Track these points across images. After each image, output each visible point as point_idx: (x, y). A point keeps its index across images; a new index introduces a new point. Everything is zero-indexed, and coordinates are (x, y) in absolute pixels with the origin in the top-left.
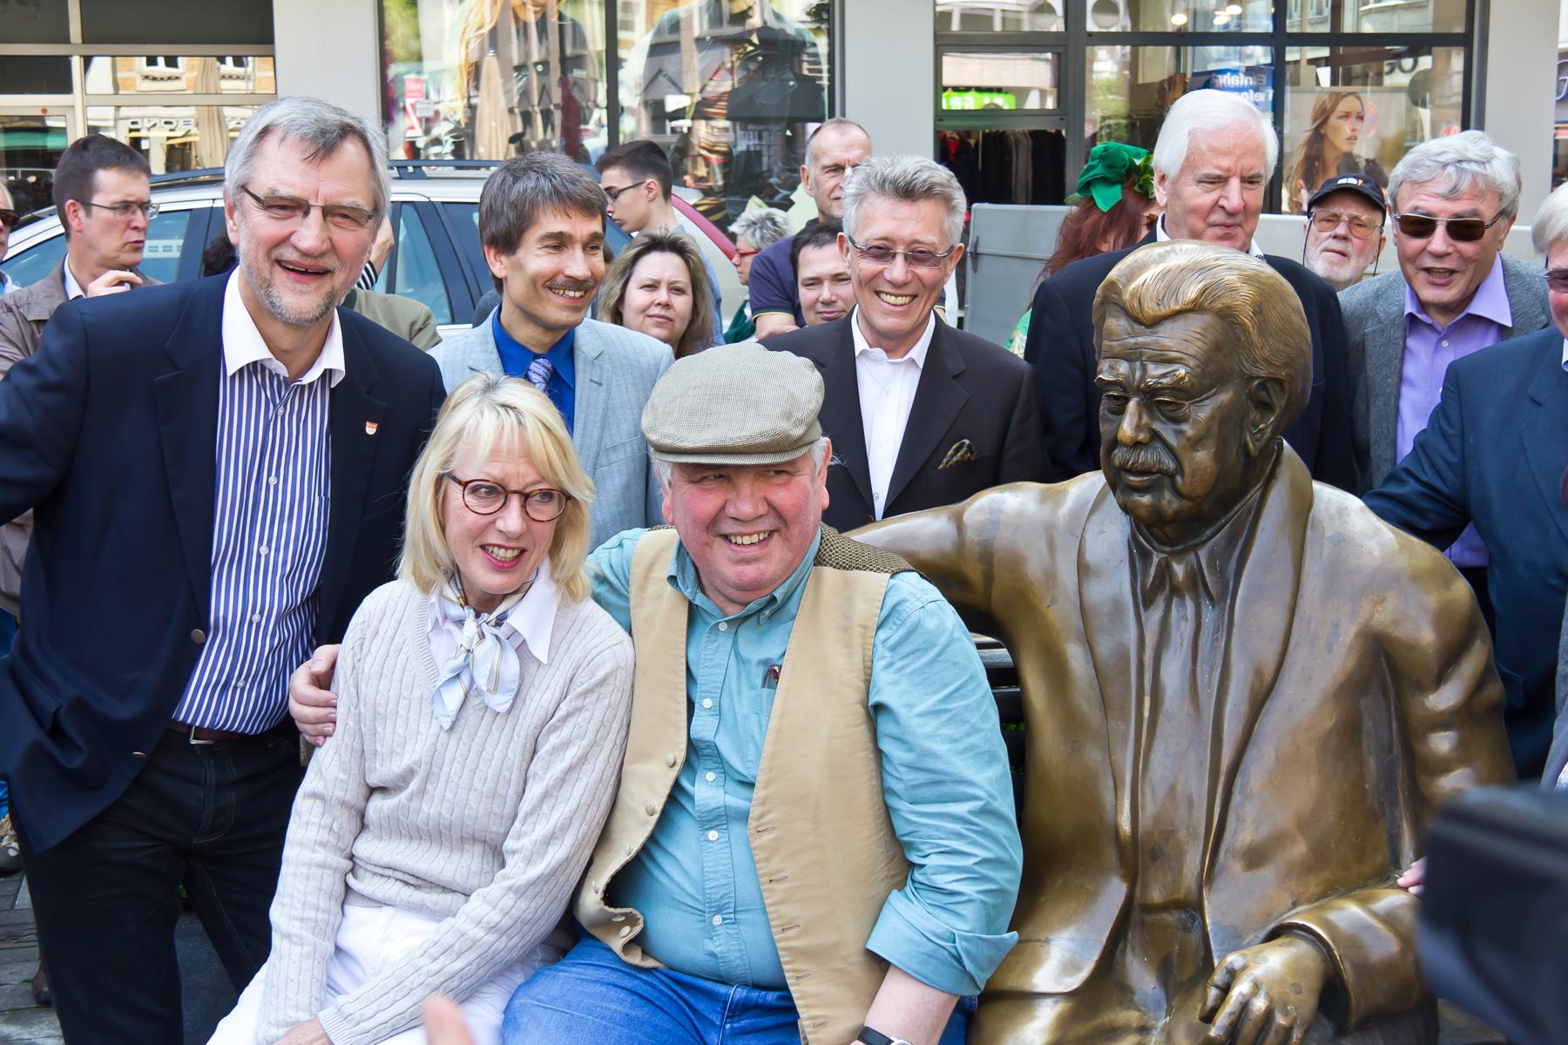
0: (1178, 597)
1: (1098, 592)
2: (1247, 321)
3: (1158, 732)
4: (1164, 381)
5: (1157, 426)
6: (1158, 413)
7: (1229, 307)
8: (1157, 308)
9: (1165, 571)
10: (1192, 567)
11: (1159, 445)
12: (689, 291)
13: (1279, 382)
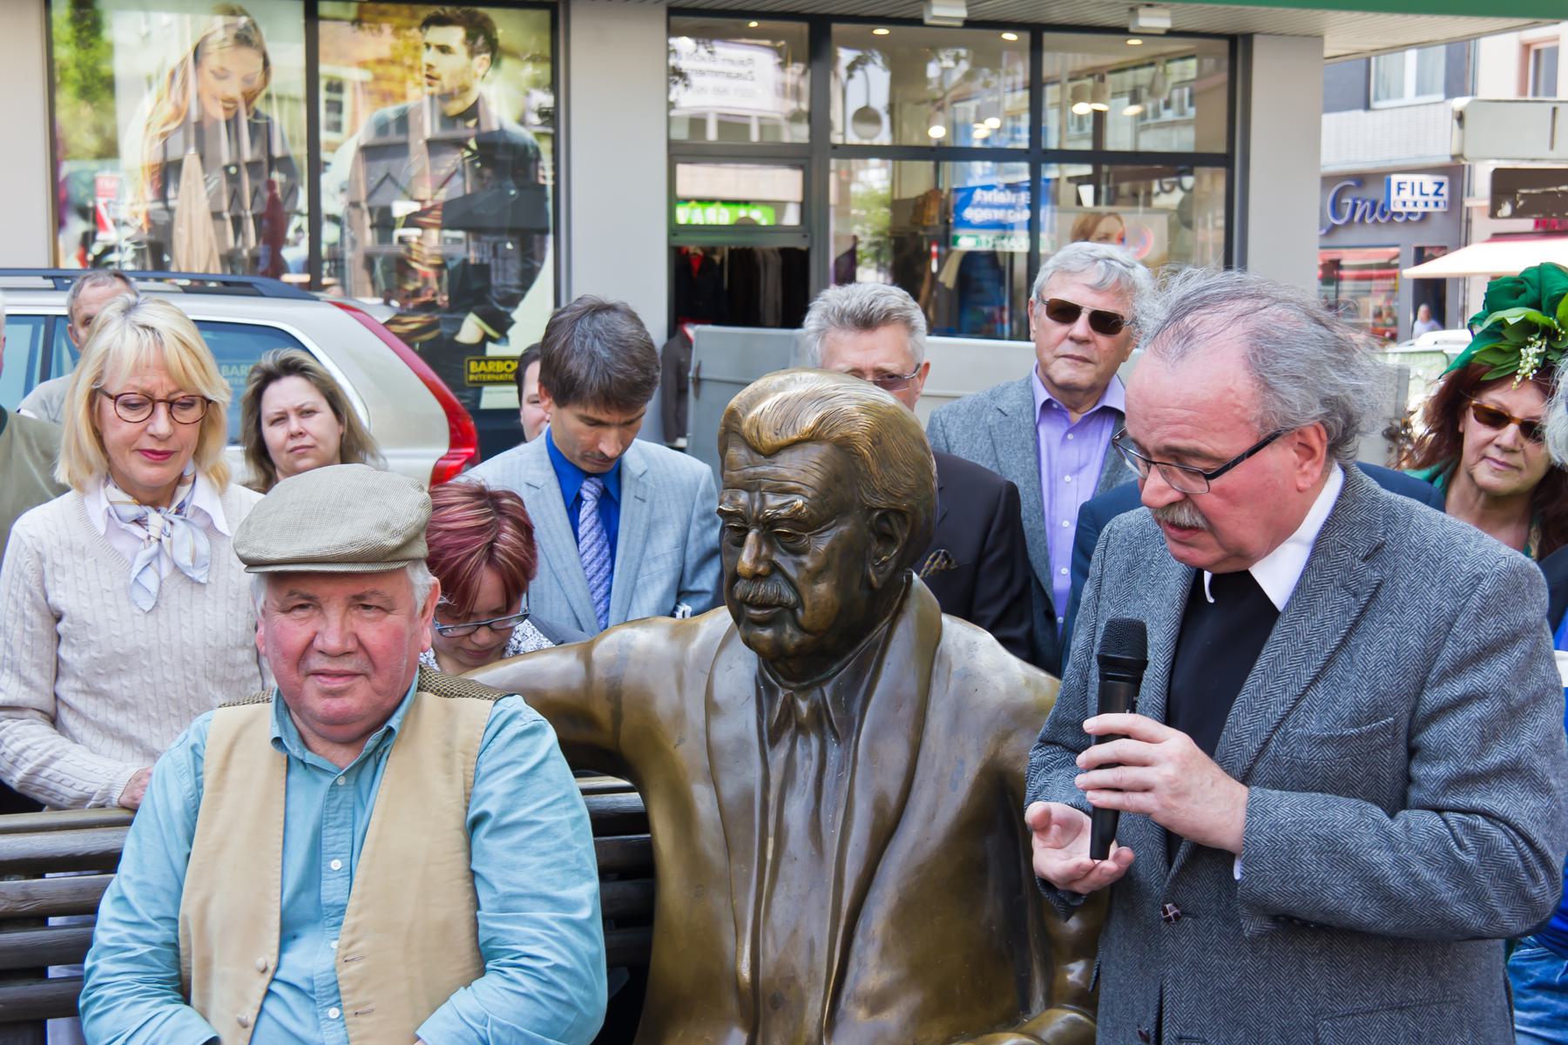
0: (803, 734)
1: (724, 731)
2: (865, 451)
3: (780, 875)
4: (782, 512)
5: (776, 558)
6: (778, 545)
7: (847, 437)
8: (774, 437)
9: (790, 708)
10: (817, 704)
11: (779, 577)
13: (899, 513)
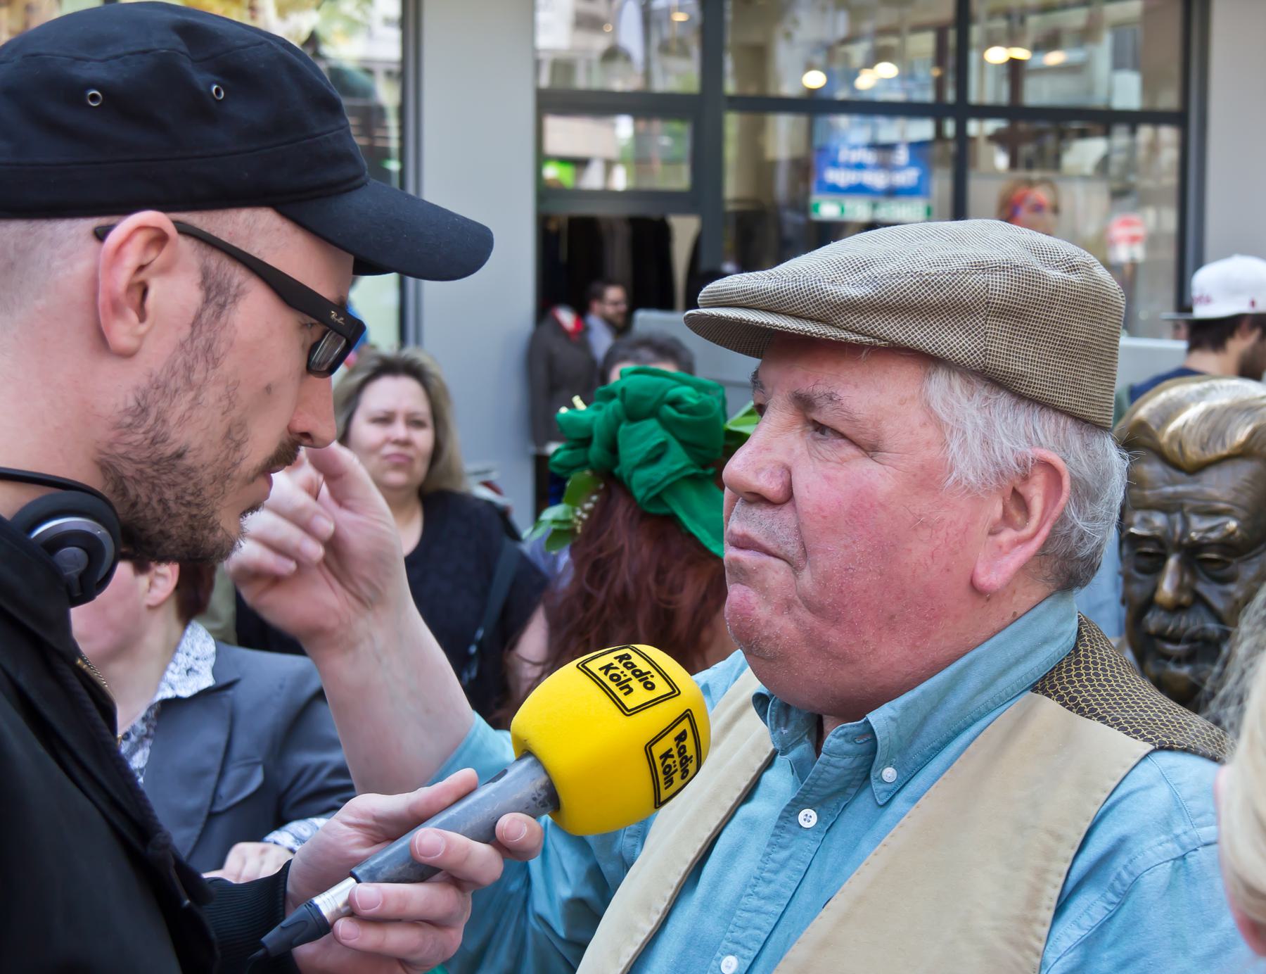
8: (1200, 452)
11: (1202, 611)
12: (429, 422)
